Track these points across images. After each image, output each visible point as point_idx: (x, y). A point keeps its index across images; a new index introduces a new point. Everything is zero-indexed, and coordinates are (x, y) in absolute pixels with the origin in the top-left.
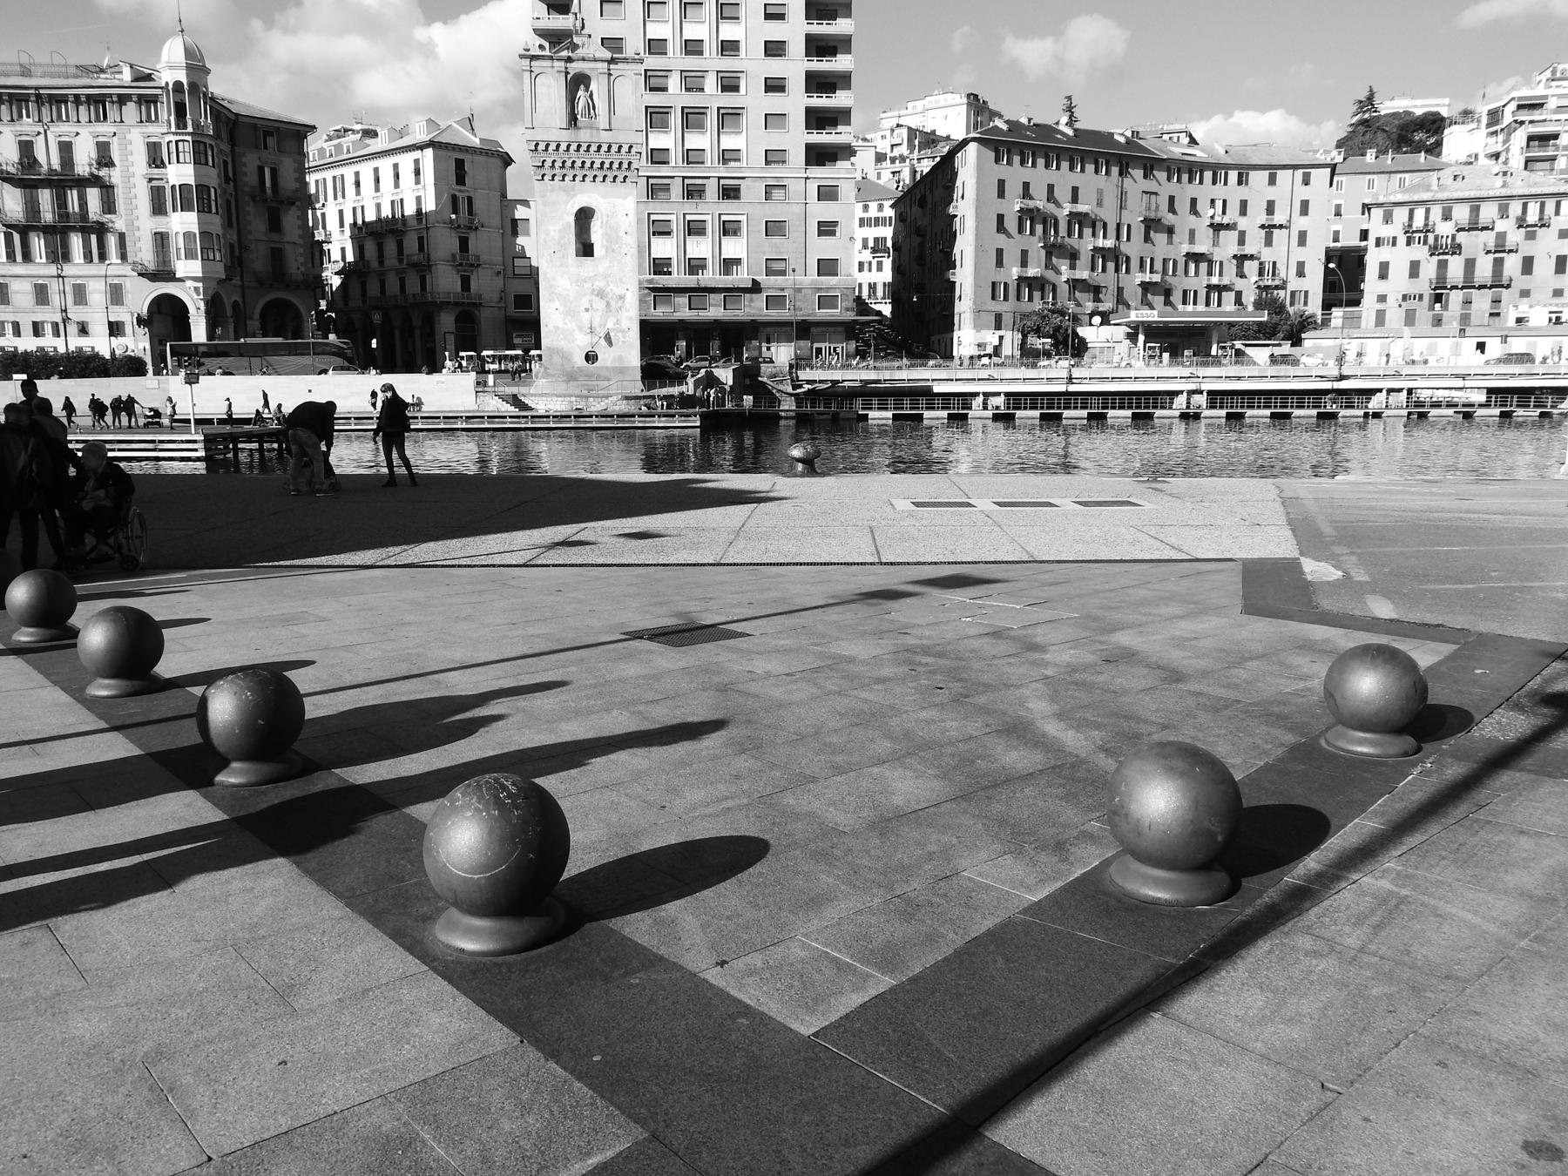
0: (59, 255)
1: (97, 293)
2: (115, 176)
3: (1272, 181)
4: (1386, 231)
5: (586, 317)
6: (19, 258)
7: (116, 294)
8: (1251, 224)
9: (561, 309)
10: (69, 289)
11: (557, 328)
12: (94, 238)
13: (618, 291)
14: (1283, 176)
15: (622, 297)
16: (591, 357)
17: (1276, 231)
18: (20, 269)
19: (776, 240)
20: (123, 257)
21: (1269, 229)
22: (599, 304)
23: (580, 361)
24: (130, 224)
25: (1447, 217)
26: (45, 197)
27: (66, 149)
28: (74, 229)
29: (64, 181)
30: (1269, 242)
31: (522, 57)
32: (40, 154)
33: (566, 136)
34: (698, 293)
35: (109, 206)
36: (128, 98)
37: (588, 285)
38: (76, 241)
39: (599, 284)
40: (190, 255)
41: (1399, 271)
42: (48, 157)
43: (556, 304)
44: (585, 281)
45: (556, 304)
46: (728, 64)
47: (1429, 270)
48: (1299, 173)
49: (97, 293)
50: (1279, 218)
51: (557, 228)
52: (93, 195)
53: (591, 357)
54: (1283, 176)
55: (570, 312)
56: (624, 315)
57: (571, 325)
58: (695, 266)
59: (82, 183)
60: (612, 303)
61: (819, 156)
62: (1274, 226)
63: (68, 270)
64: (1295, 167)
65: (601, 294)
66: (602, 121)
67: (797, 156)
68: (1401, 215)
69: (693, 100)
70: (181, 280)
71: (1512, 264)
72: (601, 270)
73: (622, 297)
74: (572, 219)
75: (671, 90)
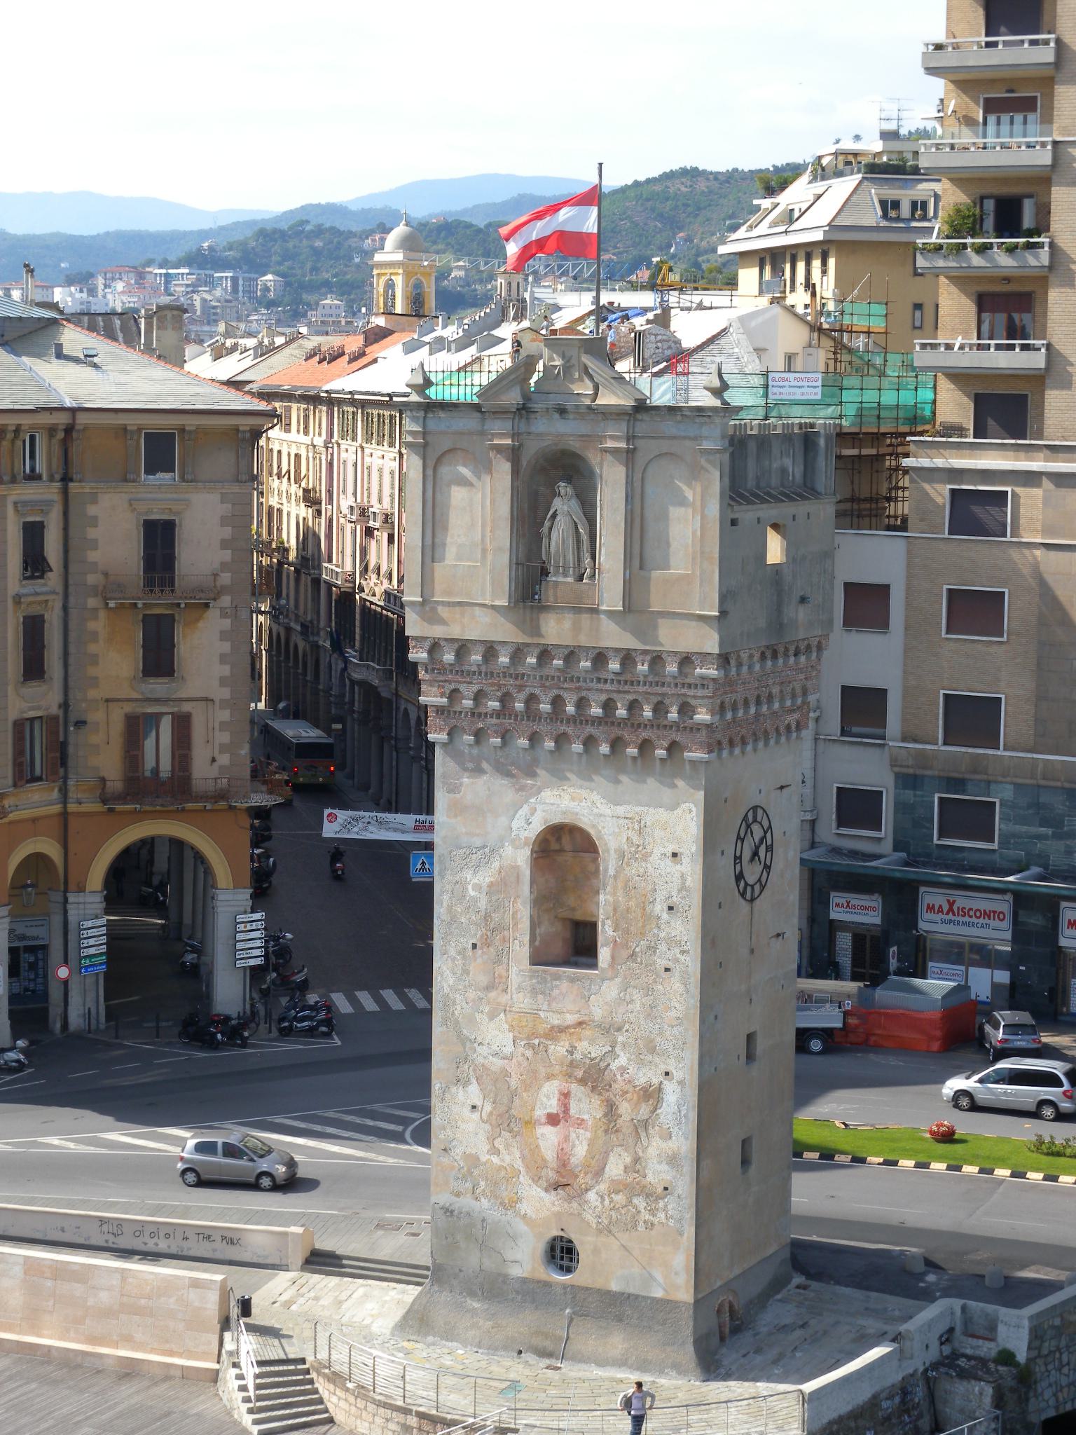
11: (473, 1160)
13: (646, 1076)
15: (652, 1095)
16: (562, 1253)
22: (586, 1107)
23: (525, 1259)
33: (504, 631)
37: (559, 1049)
39: (589, 1047)
43: (473, 1093)
44: (557, 1032)
45: (473, 1093)
51: (485, 877)
53: (562, 1253)
55: (508, 1120)
56: (655, 1148)
57: (512, 1157)
60: (624, 1108)
65: (594, 1077)
66: (610, 593)
72: (598, 1013)
73: (652, 1095)
74: (521, 858)
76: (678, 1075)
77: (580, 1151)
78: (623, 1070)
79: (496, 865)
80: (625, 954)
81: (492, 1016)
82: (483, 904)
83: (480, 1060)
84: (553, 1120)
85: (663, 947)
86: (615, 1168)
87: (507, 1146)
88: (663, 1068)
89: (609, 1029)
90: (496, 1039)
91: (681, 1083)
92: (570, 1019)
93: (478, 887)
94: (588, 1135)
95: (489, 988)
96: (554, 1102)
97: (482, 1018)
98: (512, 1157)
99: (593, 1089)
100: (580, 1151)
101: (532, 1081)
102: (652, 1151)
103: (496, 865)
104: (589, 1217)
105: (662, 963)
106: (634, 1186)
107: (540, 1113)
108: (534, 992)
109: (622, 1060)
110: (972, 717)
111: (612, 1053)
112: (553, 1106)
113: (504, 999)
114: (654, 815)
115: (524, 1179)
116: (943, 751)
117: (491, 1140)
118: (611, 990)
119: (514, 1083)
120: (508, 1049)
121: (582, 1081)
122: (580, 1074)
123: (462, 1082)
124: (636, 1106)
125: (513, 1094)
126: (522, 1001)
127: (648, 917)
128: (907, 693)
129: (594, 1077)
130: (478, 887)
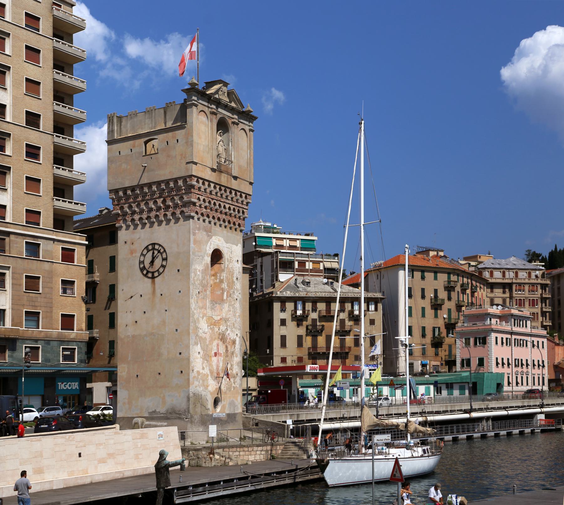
4: (283, 316)
5: (214, 359)
9: (202, 353)
11: (198, 372)
15: (234, 342)
25: (314, 309)
39: (223, 328)
41: (292, 342)
43: (198, 348)
45: (198, 348)
47: (308, 342)
55: (206, 357)
60: (229, 347)
65: (223, 338)
68: (290, 306)
71: (349, 340)
76: (239, 335)
78: (229, 334)
79: (203, 263)
80: (229, 294)
81: (203, 318)
82: (200, 277)
83: (200, 335)
84: (216, 354)
85: (236, 292)
87: (206, 366)
88: (237, 333)
89: (226, 320)
90: (203, 326)
91: (240, 337)
92: (219, 318)
93: (199, 271)
94: (222, 358)
95: (202, 308)
96: (216, 348)
97: (200, 319)
98: (206, 371)
99: (224, 342)
102: (235, 362)
103: (203, 263)
105: (236, 297)
107: (213, 353)
108: (212, 309)
109: (228, 332)
111: (227, 329)
113: (205, 312)
115: (209, 377)
117: (203, 364)
118: (226, 306)
119: (208, 343)
120: (206, 330)
121: (221, 340)
122: (220, 337)
123: (196, 344)
124: (231, 347)
125: (207, 346)
126: (209, 312)
129: (223, 338)
130: (199, 271)
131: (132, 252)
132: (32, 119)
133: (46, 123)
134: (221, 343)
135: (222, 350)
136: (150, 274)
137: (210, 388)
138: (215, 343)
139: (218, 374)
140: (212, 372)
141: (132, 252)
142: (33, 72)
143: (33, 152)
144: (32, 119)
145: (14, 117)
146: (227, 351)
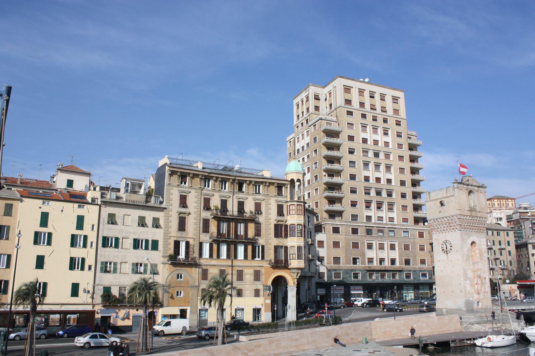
0: (232, 255)
1: (248, 275)
2: (261, 219)
3: (498, 234)
5: (476, 286)
6: (215, 255)
7: (257, 276)
8: (496, 247)
10: (235, 272)
11: (469, 292)
12: (250, 248)
13: (484, 276)
14: (502, 233)
15: (485, 278)
17: (502, 251)
18: (214, 262)
19: (407, 251)
20: (263, 258)
21: (501, 249)
24: (266, 242)
26: (224, 226)
27: (241, 205)
28: (223, 242)
29: (242, 218)
30: (501, 255)
31: (454, 183)
32: (229, 207)
34: (383, 272)
35: (258, 233)
36: (273, 184)
37: (476, 273)
38: (241, 249)
39: (479, 273)
40: (299, 257)
42: (232, 209)
44: (476, 271)
46: (389, 187)
48: (505, 232)
49: (248, 275)
50: (503, 246)
52: (251, 227)
54: (502, 233)
58: (382, 261)
59: (246, 221)
61: (417, 221)
62: (502, 249)
63: (236, 263)
64: (504, 230)
65: (479, 277)
67: (411, 221)
69: (379, 199)
70: (290, 269)
75: (371, 195)
77: (479, 288)
84: (476, 284)
86: (483, 290)
89: (480, 270)
98: (473, 291)
100: (479, 288)
101: (474, 278)
104: (481, 297)
106: (485, 292)
110: (337, 260)
112: (476, 282)
114: (482, 240)
116: (333, 266)
126: (472, 267)
127: (483, 254)
128: (327, 257)
129: (479, 277)
131: (438, 244)
132: (403, 183)
133: (408, 183)
134: (479, 279)
135: (479, 282)
136: (446, 252)
137: (475, 298)
138: (476, 279)
139: (478, 291)
140: (475, 292)
141: (438, 244)
142: (402, 165)
143: (403, 196)
144: (403, 183)
145: (395, 183)
146: (482, 282)
